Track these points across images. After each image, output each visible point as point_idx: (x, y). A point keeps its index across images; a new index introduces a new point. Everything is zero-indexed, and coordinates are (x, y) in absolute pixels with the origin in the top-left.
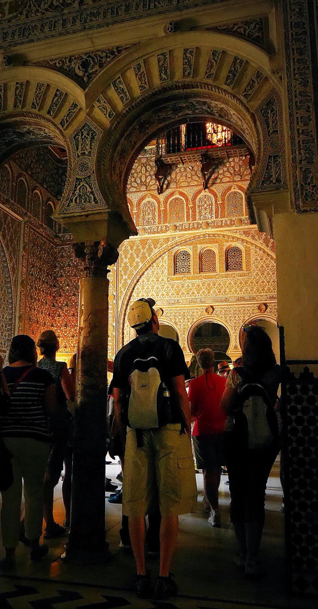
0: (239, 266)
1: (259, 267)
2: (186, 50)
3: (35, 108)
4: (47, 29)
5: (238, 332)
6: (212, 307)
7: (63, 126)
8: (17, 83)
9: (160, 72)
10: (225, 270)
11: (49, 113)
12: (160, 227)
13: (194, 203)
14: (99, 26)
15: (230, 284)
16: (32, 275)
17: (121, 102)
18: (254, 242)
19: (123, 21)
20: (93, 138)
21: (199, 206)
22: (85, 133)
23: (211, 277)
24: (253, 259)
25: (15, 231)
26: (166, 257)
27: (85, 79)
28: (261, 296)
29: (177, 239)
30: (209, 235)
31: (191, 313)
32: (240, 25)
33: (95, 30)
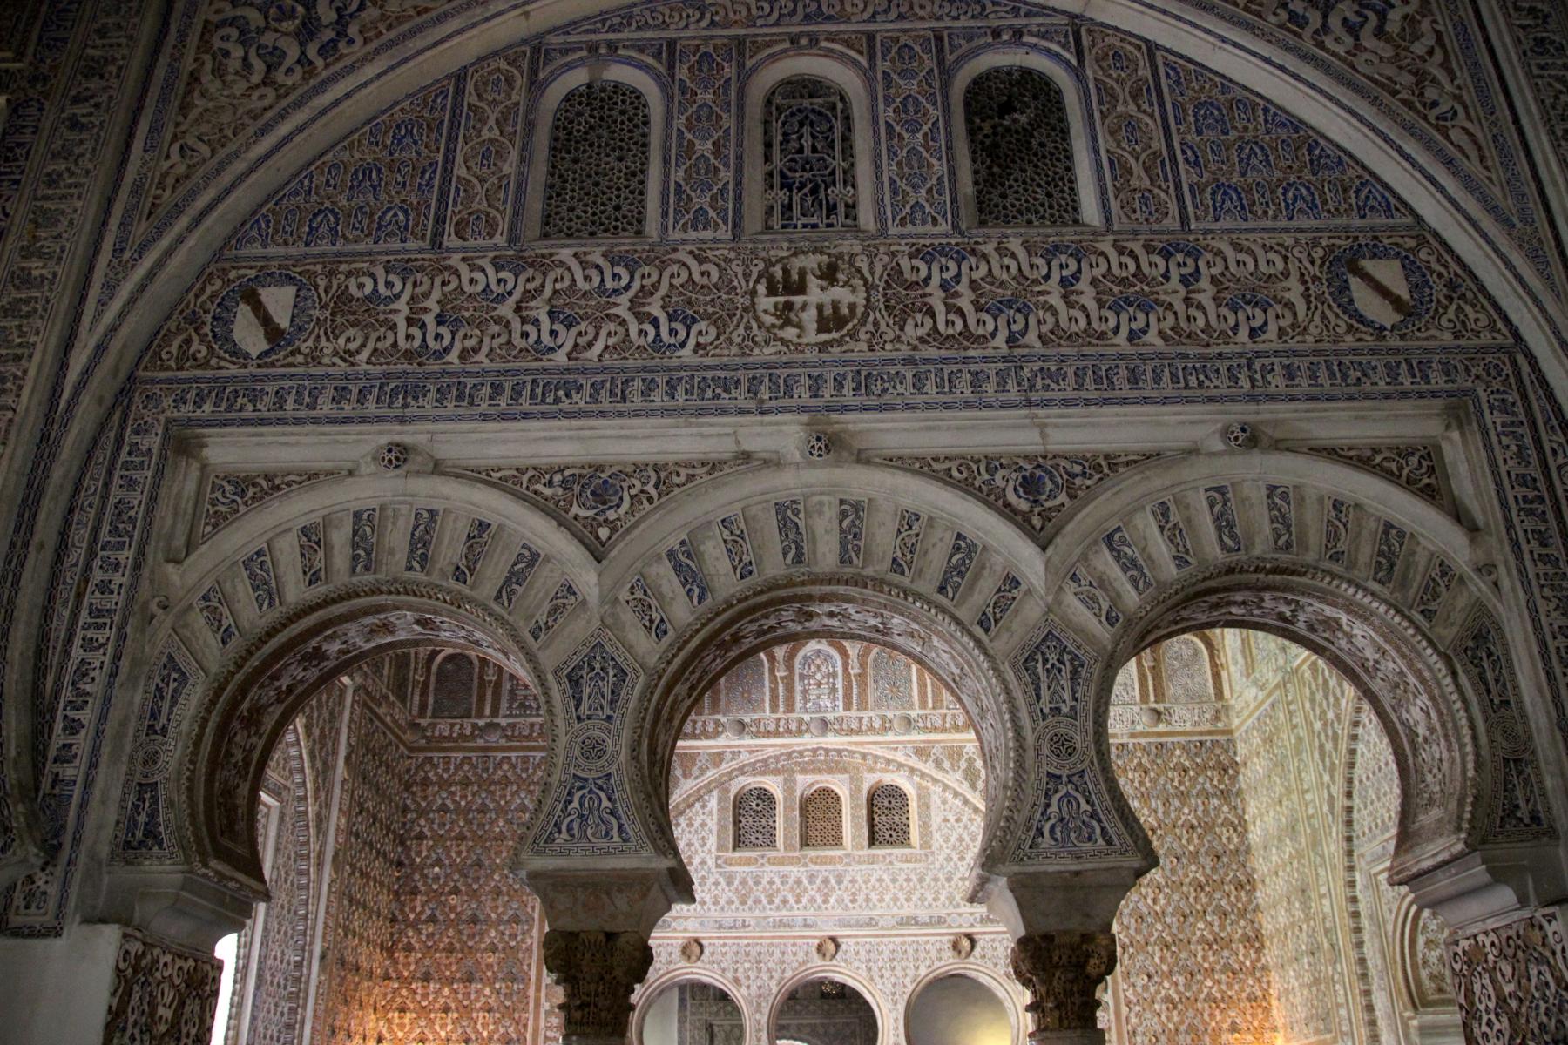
0: (900, 836)
1: (953, 839)
2: (1272, 489)
3: (903, 573)
4: (930, 387)
5: (901, 1007)
6: (833, 939)
7: (987, 630)
8: (842, 502)
9: (1219, 529)
10: (866, 843)
11: (942, 589)
12: (699, 724)
13: (790, 668)
14: (1065, 403)
15: (880, 880)
16: (357, 836)
17: (1133, 593)
18: (939, 775)
19: (1124, 402)
20: (1075, 673)
21: (802, 677)
22: (1053, 658)
23: (831, 860)
24: (936, 820)
25: (332, 714)
26: (713, 803)
27: (1037, 521)
28: (960, 915)
29: (745, 758)
30: (827, 751)
31: (777, 955)
32: (1387, 454)
33: (1056, 411)
